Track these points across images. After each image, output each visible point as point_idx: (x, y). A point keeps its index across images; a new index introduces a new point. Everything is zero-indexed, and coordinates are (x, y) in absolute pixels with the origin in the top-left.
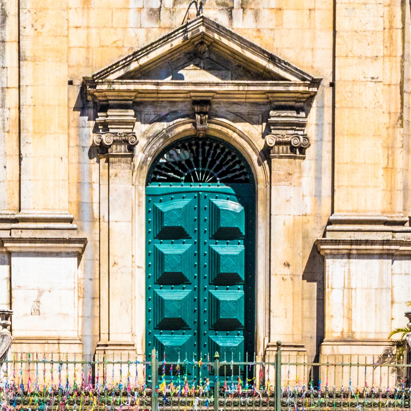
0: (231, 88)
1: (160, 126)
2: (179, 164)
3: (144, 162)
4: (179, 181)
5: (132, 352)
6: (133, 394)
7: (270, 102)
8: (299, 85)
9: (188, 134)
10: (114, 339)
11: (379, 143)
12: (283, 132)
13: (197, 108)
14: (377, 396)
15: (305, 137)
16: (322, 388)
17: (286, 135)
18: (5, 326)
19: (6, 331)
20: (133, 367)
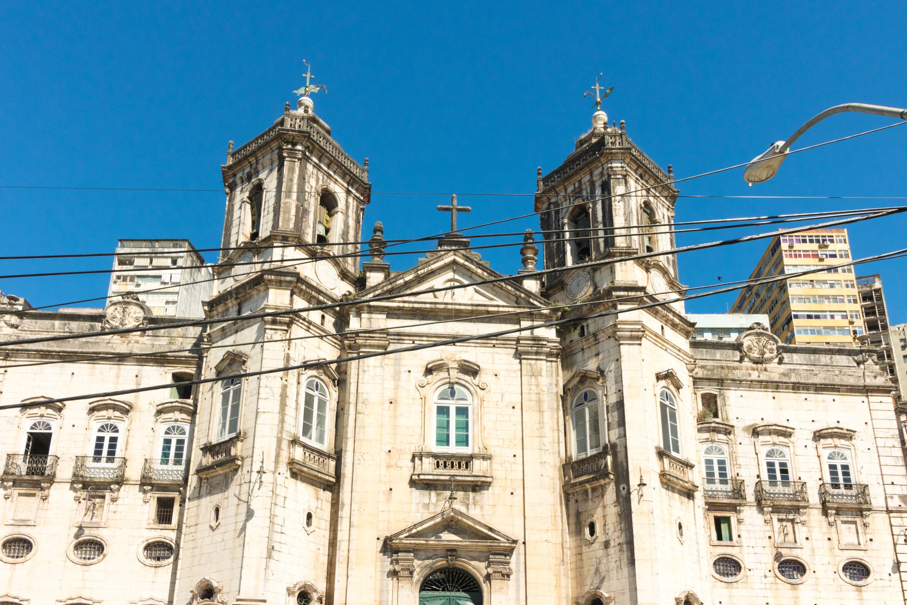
0: (468, 543)
1: (427, 562)
2: (438, 581)
3: (418, 580)
4: (439, 590)
8: (506, 543)
9: (444, 566)
12: (498, 566)
13: (449, 553)
15: (510, 569)
17: (500, 568)
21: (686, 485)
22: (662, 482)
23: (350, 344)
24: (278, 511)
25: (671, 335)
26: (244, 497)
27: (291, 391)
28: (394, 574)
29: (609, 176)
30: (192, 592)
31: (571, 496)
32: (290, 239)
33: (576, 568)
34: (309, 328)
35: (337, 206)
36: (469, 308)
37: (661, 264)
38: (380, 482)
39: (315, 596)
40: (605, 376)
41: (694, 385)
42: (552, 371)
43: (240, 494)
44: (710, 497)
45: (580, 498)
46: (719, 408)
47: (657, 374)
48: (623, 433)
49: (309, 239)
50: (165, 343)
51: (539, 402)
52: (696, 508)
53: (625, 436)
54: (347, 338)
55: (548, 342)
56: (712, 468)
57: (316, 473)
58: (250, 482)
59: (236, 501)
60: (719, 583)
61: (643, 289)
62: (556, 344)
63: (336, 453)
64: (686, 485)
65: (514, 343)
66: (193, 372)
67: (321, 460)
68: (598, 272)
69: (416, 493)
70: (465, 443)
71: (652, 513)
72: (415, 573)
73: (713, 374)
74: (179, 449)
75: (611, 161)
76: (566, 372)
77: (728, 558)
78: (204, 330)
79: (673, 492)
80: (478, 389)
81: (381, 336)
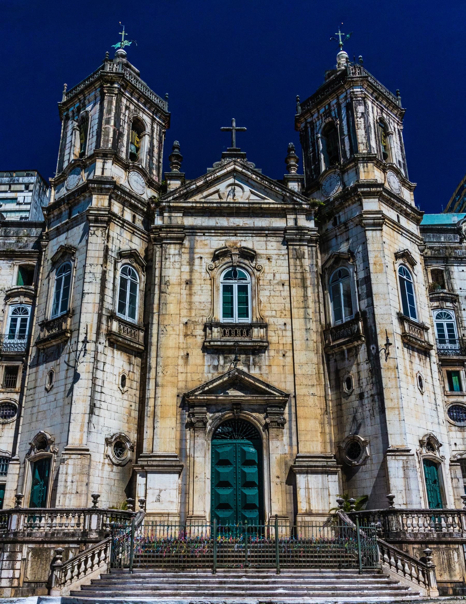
0: (249, 398)
1: (217, 414)
3: (210, 430)
4: (227, 439)
5: (204, 521)
6: (204, 542)
7: (267, 404)
9: (230, 418)
10: (196, 513)
11: (317, 422)
14: (327, 543)
15: (284, 419)
16: (299, 539)
17: (276, 418)
18: (142, 507)
19: (142, 510)
20: (204, 528)
21: (423, 344)
22: (403, 342)
23: (155, 237)
24: (99, 374)
25: (404, 222)
26: (72, 363)
27: (110, 276)
28: (190, 425)
29: (352, 98)
30: (30, 444)
31: (331, 357)
32: (109, 155)
33: (337, 417)
34: (124, 225)
35: (145, 130)
36: (247, 206)
37: (394, 166)
38: (179, 348)
39: (128, 445)
40: (354, 257)
41: (425, 263)
42: (313, 254)
43: (69, 361)
44: (442, 354)
45: (338, 357)
46: (446, 281)
47: (395, 254)
48: (371, 302)
49: (123, 155)
50: (14, 242)
51: (303, 279)
52: (432, 364)
53: (373, 304)
54: (153, 233)
55: (309, 231)
56: (443, 331)
57: (129, 343)
58: (77, 351)
59: (65, 367)
60: (453, 428)
61: (382, 185)
62: (315, 233)
63: (144, 325)
64: (423, 344)
65: (282, 232)
66: (35, 264)
67: (133, 331)
68: (346, 174)
69: (207, 357)
70: (245, 315)
71: (397, 368)
72: (208, 424)
73: (439, 254)
74: (23, 325)
75: (353, 87)
76: (323, 255)
77: (460, 406)
78: (44, 230)
79: (413, 350)
80: (255, 271)
81: (179, 230)
